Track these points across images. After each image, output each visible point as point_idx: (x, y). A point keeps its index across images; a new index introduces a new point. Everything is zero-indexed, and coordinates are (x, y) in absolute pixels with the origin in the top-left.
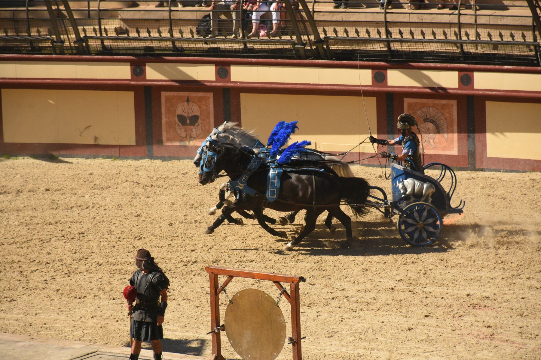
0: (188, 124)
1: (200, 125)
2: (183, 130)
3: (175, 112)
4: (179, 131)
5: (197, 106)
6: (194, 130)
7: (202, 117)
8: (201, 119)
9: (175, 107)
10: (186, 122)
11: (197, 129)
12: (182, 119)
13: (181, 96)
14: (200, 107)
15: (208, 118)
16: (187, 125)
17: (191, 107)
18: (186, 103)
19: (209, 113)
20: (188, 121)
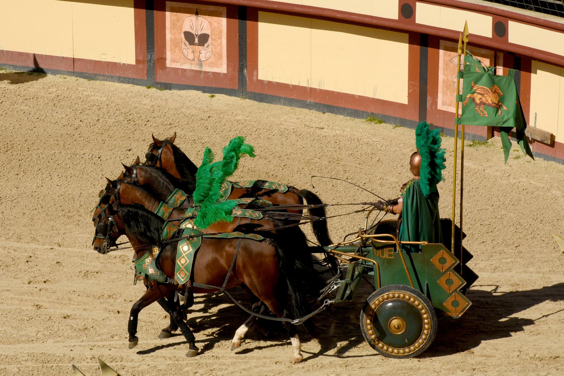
0: (196, 43)
1: (211, 47)
2: (191, 51)
4: (185, 51)
5: (207, 22)
6: (203, 52)
7: (213, 37)
9: (181, 22)
10: (194, 40)
11: (206, 51)
12: (189, 37)
14: (210, 23)
15: (220, 38)
19: (221, 32)
20: (196, 41)
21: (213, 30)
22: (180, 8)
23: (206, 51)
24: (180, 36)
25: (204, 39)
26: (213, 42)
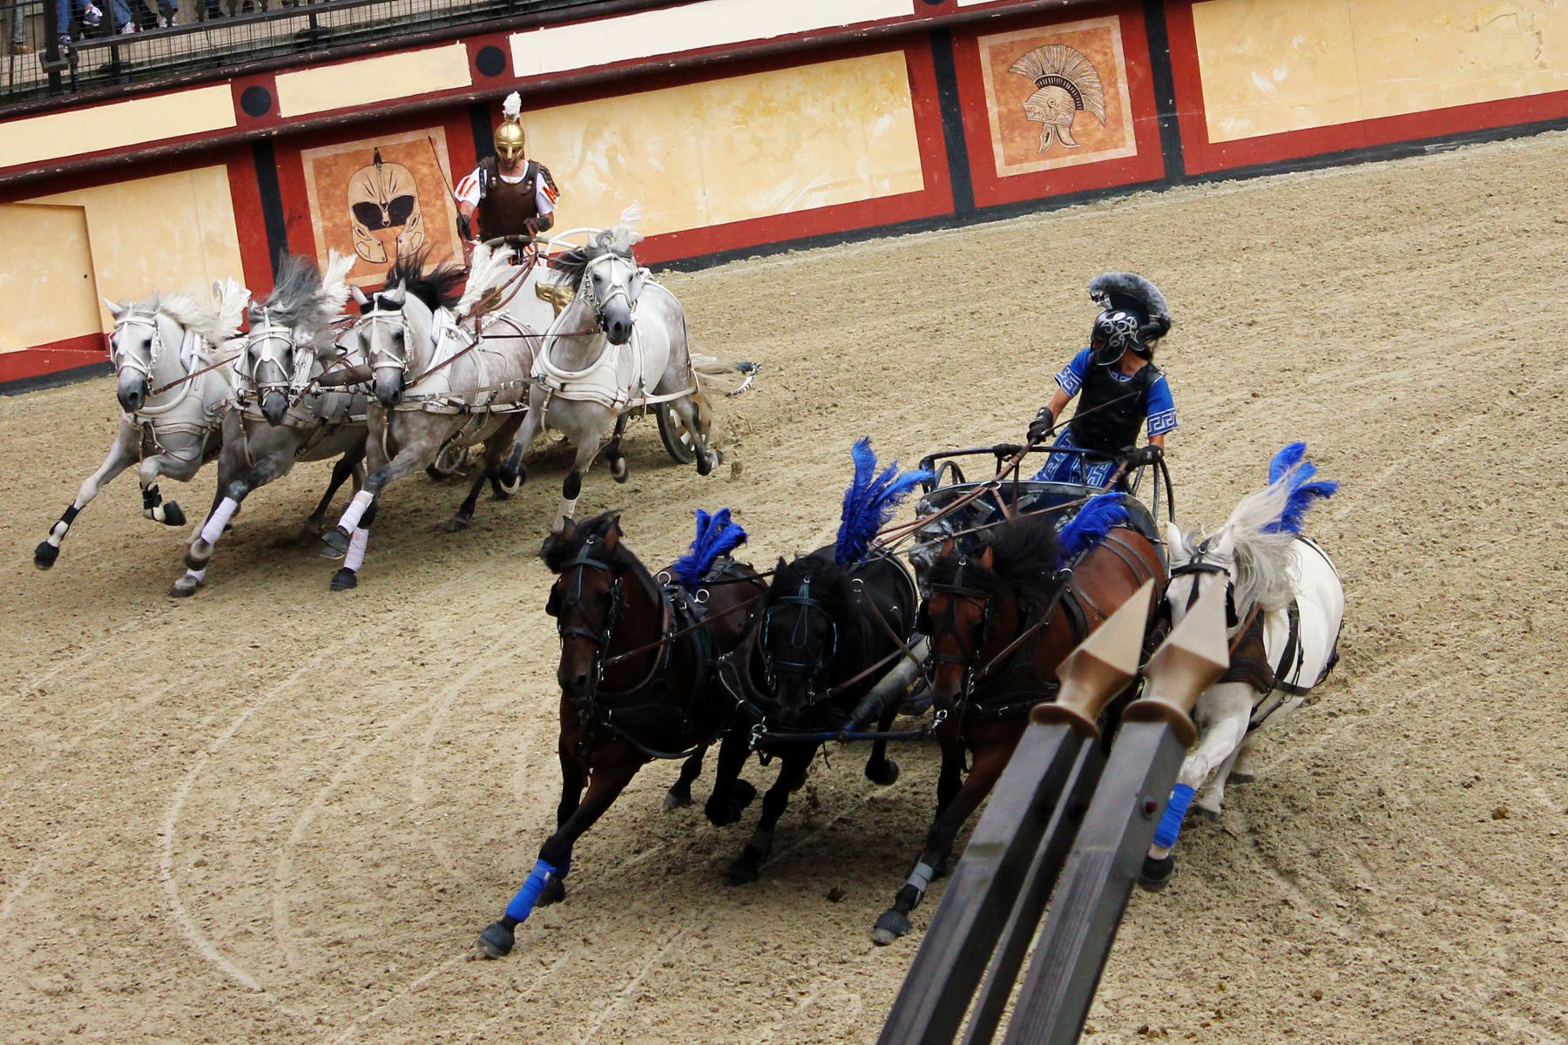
1: (421, 221)
2: (375, 242)
3: (345, 199)
4: (362, 249)
5: (405, 170)
7: (423, 198)
8: (424, 204)
9: (343, 186)
11: (412, 234)
12: (368, 214)
13: (356, 153)
14: (412, 171)
16: (382, 227)
17: (388, 177)
18: (372, 170)
20: (386, 217)
21: (420, 184)
22: (337, 155)
23: (412, 234)
24: (345, 219)
25: (401, 209)
26: (424, 209)
